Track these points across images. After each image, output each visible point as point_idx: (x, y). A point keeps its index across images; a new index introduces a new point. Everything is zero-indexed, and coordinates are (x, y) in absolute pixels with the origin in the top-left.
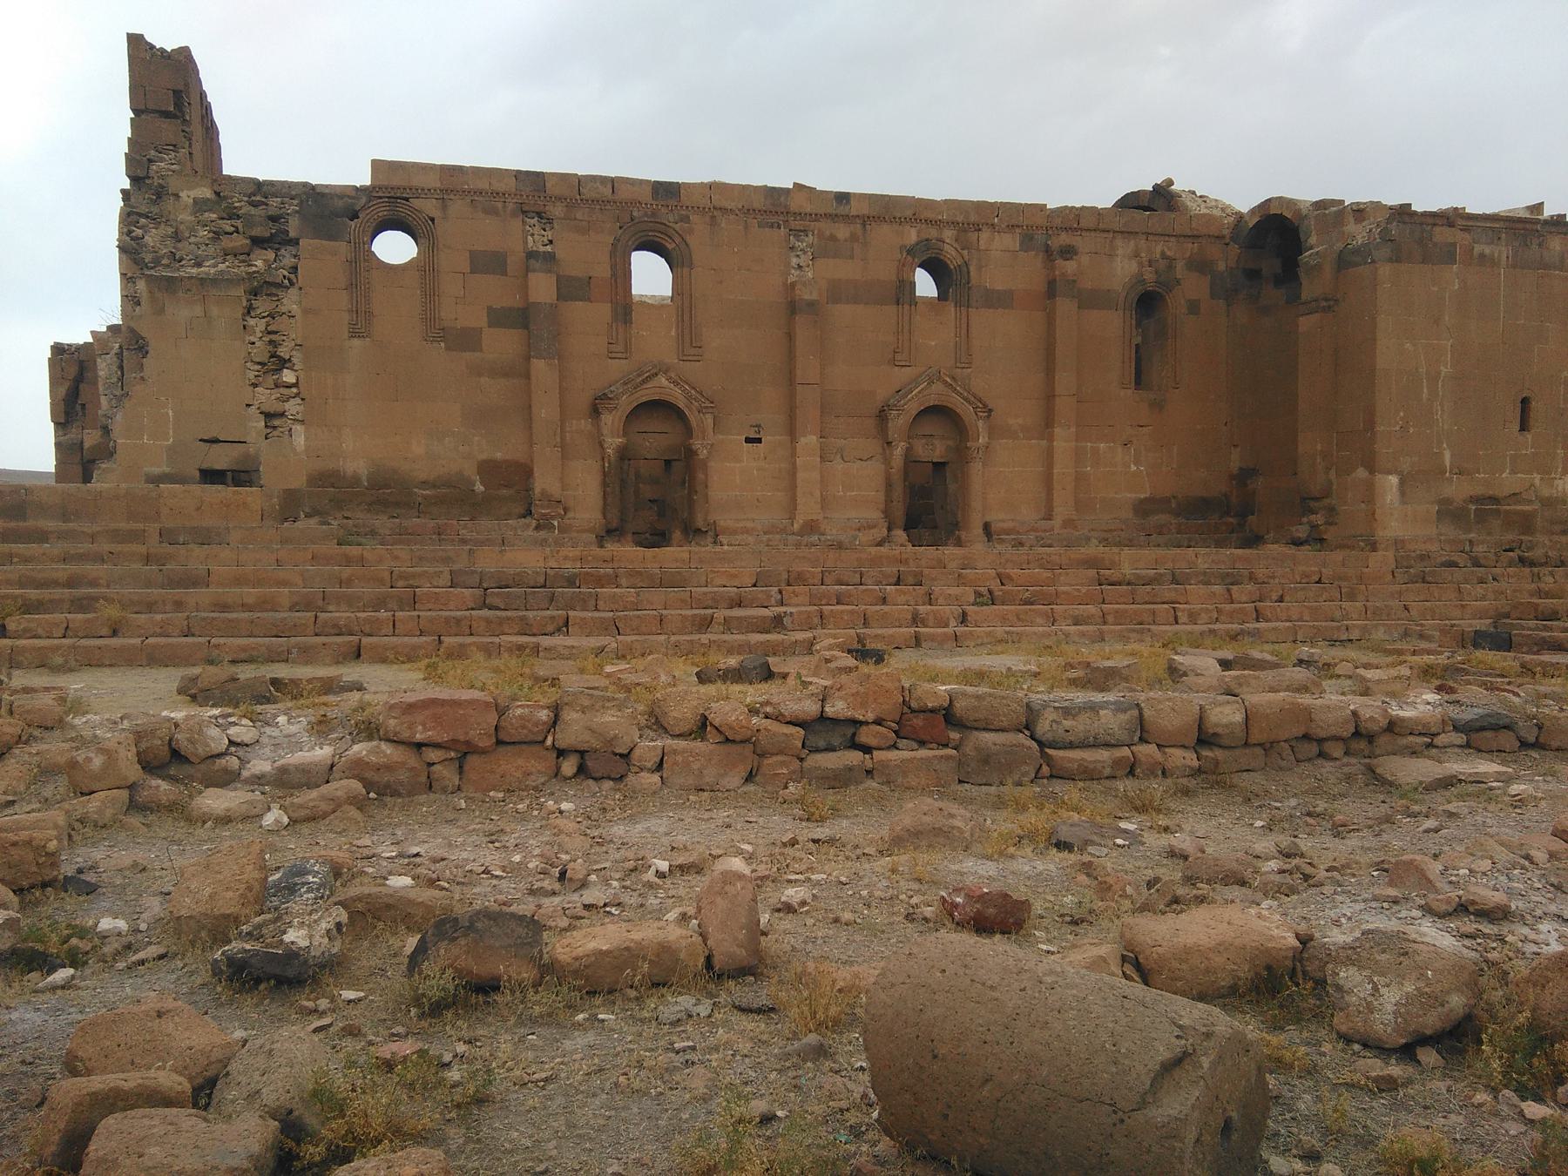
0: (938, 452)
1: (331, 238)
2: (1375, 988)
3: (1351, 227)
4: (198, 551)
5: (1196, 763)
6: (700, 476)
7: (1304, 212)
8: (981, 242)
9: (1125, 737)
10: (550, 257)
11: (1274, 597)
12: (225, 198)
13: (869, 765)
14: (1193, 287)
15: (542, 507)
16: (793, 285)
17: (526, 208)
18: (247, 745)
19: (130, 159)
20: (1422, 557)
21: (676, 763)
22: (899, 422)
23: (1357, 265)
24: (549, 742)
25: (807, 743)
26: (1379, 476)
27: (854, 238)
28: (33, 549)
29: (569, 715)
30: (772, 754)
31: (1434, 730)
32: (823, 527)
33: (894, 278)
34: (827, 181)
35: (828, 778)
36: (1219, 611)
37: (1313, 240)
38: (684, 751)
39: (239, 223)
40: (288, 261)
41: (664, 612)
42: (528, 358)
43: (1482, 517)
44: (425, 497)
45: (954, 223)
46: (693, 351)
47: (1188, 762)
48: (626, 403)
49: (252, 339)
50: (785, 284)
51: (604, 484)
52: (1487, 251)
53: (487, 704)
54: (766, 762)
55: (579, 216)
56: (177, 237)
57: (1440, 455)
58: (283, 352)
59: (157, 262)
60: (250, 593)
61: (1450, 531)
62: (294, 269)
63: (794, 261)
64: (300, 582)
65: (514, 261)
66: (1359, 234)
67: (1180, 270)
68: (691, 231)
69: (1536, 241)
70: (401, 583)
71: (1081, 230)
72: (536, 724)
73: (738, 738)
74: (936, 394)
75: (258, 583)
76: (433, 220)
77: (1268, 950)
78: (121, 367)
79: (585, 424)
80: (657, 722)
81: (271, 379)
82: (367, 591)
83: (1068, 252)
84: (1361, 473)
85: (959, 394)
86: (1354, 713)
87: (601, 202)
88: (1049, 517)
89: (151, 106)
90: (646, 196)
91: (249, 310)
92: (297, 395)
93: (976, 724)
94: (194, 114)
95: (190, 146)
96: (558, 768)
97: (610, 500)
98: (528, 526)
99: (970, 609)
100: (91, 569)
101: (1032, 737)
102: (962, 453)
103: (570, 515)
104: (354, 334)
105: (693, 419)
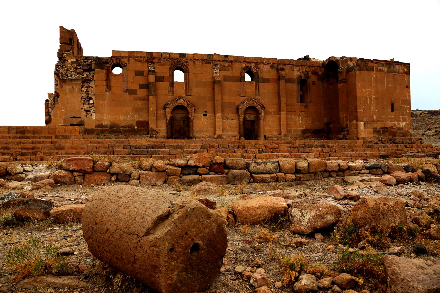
0: (252, 118)
1: (102, 69)
2: (302, 214)
3: (349, 63)
4: (63, 141)
5: (294, 178)
6: (191, 124)
7: (338, 59)
8: (261, 67)
9: (274, 170)
10: (154, 72)
11: (334, 151)
12: (78, 61)
13: (201, 179)
14: (313, 78)
15: (151, 132)
16: (214, 77)
18: (29, 171)
19: (58, 54)
20: (370, 142)
21: (143, 177)
22: (242, 110)
23: (351, 71)
24: (108, 171)
25: (183, 172)
26: (359, 122)
27: (229, 66)
28: (26, 140)
29: (114, 164)
30: (172, 175)
31: (360, 169)
32: (223, 136)
33: (240, 75)
35: (188, 182)
36: (320, 154)
37: (341, 66)
38: (145, 174)
39: (81, 66)
40: (92, 74)
41: (176, 155)
42: (148, 96)
43: (384, 132)
45: (254, 63)
46: (189, 93)
47: (292, 177)
48: (172, 106)
49: (83, 93)
50: (212, 77)
51: (167, 126)
52: (381, 68)
53: (90, 160)
54: (170, 177)
55: (161, 62)
56: (67, 70)
57: (373, 117)
58: (90, 96)
60: (74, 151)
61: (376, 136)
62: (93, 76)
63: (215, 71)
64: (87, 148)
65: (145, 73)
66: (351, 64)
67: (310, 73)
68: (189, 65)
69: (392, 66)
70: (111, 148)
71: (286, 64)
72: (104, 166)
73: (161, 170)
74: (251, 103)
75: (77, 148)
76: (126, 64)
77: (275, 208)
78: (54, 101)
79: (162, 112)
80: (140, 167)
81: (87, 102)
82: (102, 150)
83: (283, 69)
84: (355, 122)
85: (257, 103)
86: (339, 164)
87: (166, 59)
88: (281, 134)
89: (64, 42)
91: (82, 86)
92: (93, 106)
93: (232, 168)
94: (75, 44)
95: (73, 51)
96: (111, 178)
97: (168, 130)
98: (148, 137)
99: (257, 154)
100: (38, 145)
101: (249, 171)
102: (258, 118)
103: (159, 134)
104: (107, 91)
105: (189, 109)
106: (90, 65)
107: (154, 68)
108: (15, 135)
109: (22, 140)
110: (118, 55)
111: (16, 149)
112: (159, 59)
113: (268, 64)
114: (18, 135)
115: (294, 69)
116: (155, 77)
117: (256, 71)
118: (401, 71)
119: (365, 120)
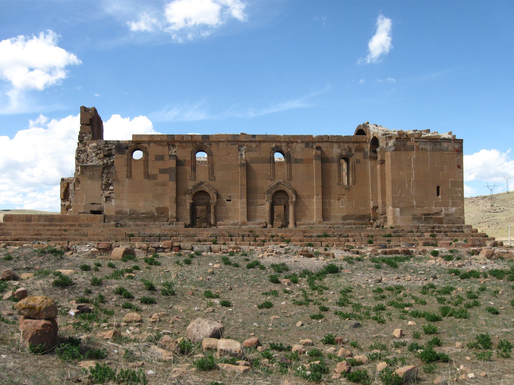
1: (122, 154)
17: (169, 144)
34: (250, 132)
43: (426, 220)
44: (142, 217)
45: (285, 142)
52: (424, 147)
57: (412, 203)
59: (83, 161)
61: (416, 223)
67: (353, 150)
76: (146, 148)
78: (75, 187)
85: (286, 186)
89: (85, 123)
90: (200, 139)
91: (103, 172)
105: (211, 195)
106: (110, 150)
107: (175, 152)
108: (44, 223)
109: (51, 228)
110: (139, 139)
111: (46, 235)
112: (180, 142)
113: (302, 142)
114: (47, 223)
115: (333, 146)
116: (175, 161)
117: (287, 151)
118: (451, 148)
119: (402, 206)
